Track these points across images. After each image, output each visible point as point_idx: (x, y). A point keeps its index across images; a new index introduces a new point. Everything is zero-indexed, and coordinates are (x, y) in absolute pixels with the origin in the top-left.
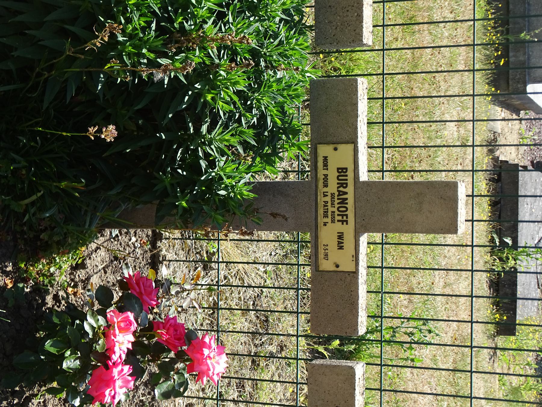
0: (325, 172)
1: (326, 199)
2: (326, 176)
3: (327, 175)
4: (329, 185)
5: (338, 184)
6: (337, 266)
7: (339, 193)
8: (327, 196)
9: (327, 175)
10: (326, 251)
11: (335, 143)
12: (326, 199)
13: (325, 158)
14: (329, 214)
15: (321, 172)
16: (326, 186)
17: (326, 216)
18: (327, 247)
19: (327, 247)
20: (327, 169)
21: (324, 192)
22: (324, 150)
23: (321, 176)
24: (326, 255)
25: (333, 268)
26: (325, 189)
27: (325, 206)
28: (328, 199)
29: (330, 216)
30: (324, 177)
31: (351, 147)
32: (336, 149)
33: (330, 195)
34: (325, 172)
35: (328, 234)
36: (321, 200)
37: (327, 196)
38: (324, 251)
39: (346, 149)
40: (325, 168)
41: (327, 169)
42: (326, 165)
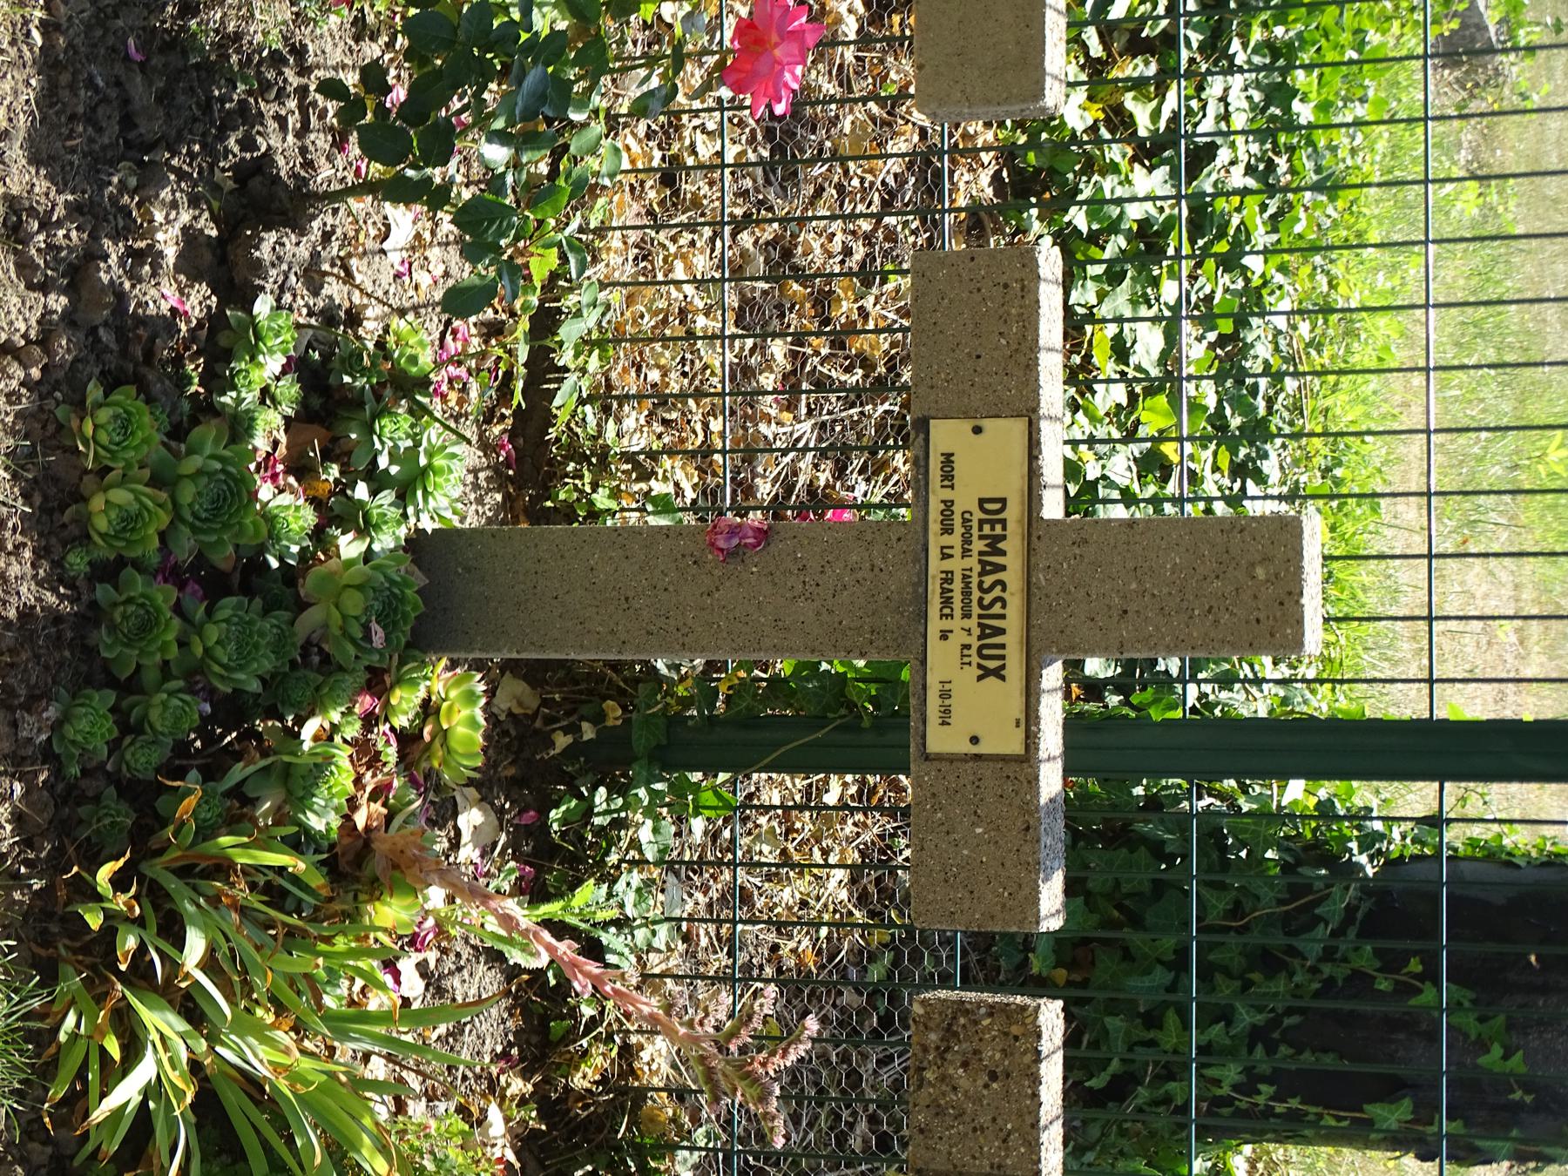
0: (947, 494)
1: (948, 565)
2: (949, 504)
7: (983, 568)
10: (947, 702)
11: (976, 414)
12: (948, 565)
13: (948, 459)
16: (947, 530)
20: (952, 487)
24: (946, 711)
25: (967, 748)
26: (947, 540)
27: (945, 580)
29: (958, 613)
30: (942, 506)
31: (1018, 427)
32: (977, 430)
34: (947, 494)
36: (935, 565)
38: (940, 701)
39: (1006, 432)
41: (952, 487)
42: (948, 477)
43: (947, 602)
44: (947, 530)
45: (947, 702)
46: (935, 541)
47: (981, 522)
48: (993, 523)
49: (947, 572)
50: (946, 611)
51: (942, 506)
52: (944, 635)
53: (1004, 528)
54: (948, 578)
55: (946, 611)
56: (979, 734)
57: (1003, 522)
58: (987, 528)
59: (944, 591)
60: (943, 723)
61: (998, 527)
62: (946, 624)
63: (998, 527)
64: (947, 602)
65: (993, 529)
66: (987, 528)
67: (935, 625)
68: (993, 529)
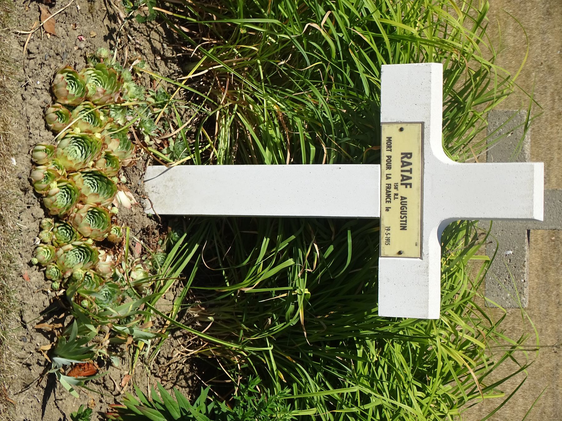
0: (389, 153)
1: (389, 181)
2: (389, 157)
3: (391, 156)
4: (392, 167)
8: (390, 178)
9: (391, 156)
10: (388, 236)
12: (389, 181)
13: (389, 139)
14: (392, 197)
16: (389, 167)
18: (389, 232)
20: (391, 150)
21: (387, 175)
24: (388, 240)
26: (388, 172)
30: (387, 158)
32: (401, 130)
34: (389, 153)
37: (390, 178)
38: (385, 236)
40: (388, 149)
41: (391, 150)
42: (389, 146)
43: (388, 196)
44: (389, 167)
45: (388, 236)
49: (388, 184)
50: (388, 200)
51: (387, 158)
52: (387, 209)
55: (388, 200)
59: (387, 192)
62: (388, 205)
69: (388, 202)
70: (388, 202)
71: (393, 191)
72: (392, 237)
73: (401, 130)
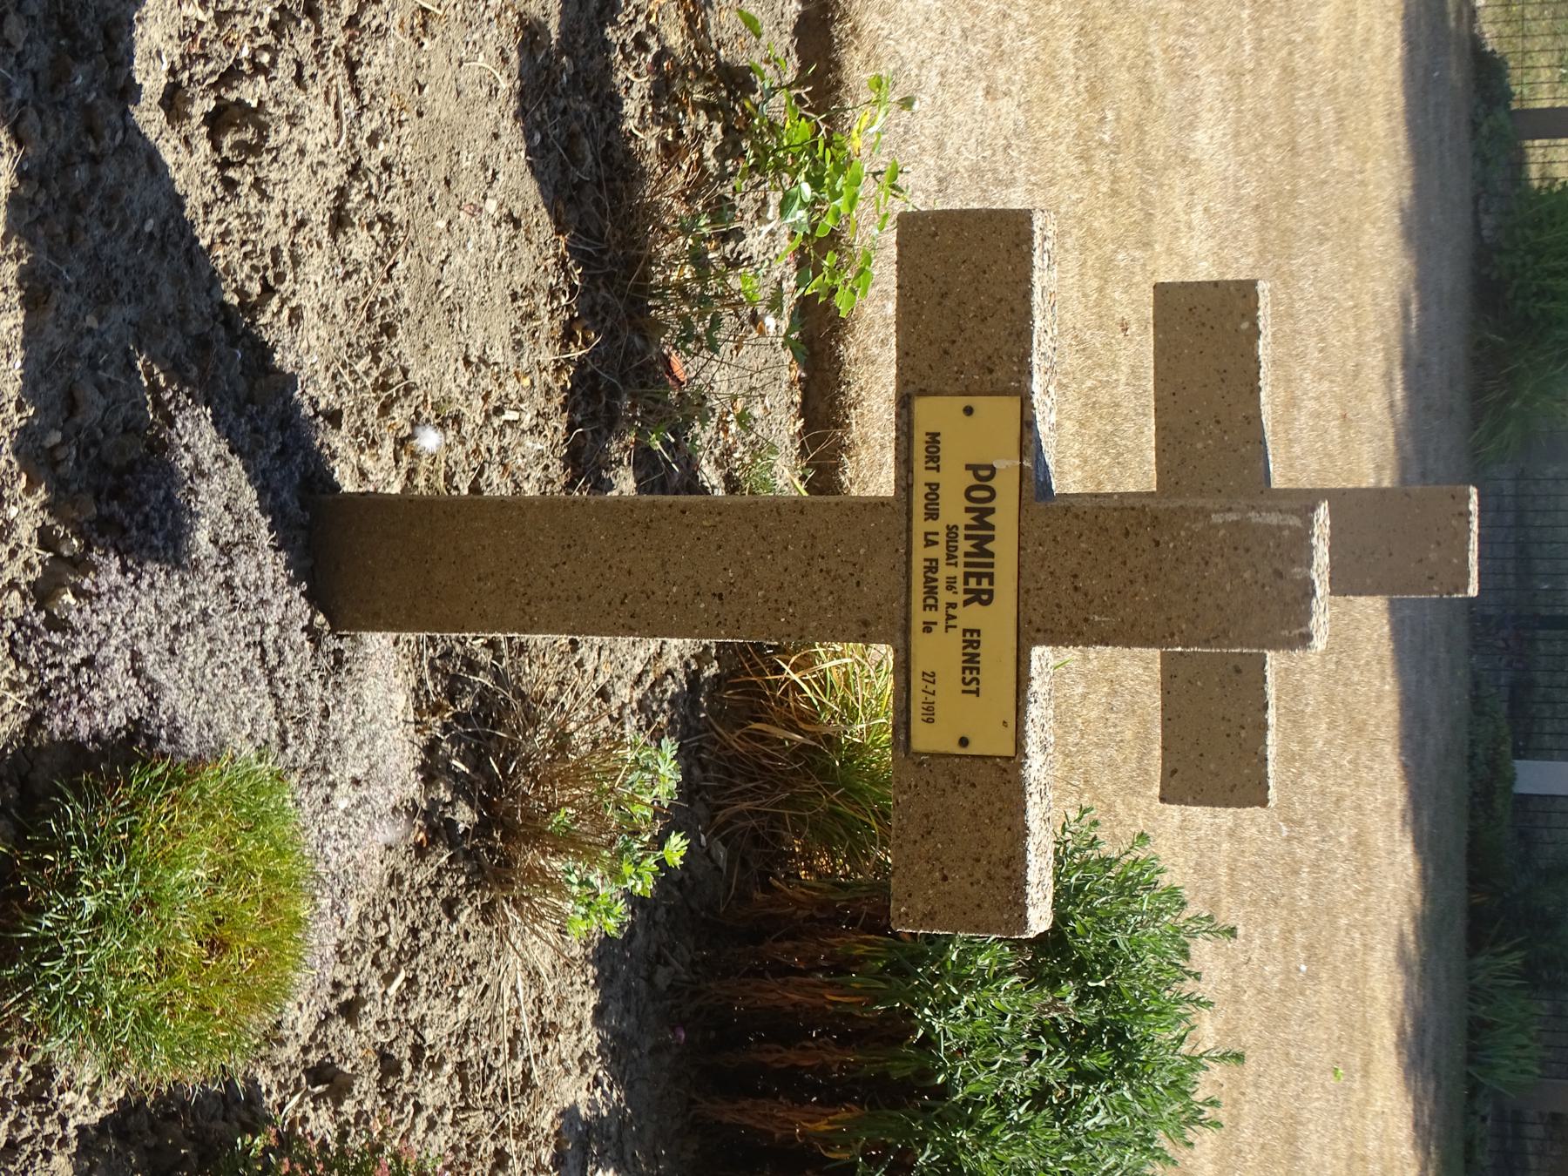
0: (933, 477)
1: (933, 552)
2: (933, 487)
5: (968, 510)
6: (964, 742)
8: (936, 543)
10: (931, 698)
12: (933, 552)
13: (934, 438)
15: (922, 476)
16: (932, 514)
17: (931, 603)
18: (931, 688)
19: (931, 688)
20: (938, 469)
21: (927, 534)
22: (929, 412)
23: (919, 492)
26: (931, 526)
28: (939, 552)
30: (927, 490)
33: (942, 539)
34: (933, 477)
35: (937, 652)
36: (920, 554)
37: (936, 543)
40: (931, 464)
41: (938, 469)
42: (933, 458)
43: (931, 591)
45: (931, 698)
46: (920, 525)
47: (967, 576)
48: (979, 577)
49: (931, 560)
52: (928, 628)
53: (991, 583)
54: (932, 565)
56: (969, 736)
57: (991, 577)
58: (973, 583)
59: (928, 580)
60: (930, 721)
61: (985, 584)
62: (930, 616)
63: (985, 582)
64: (931, 591)
65: (979, 583)
66: (973, 583)
67: (919, 616)
68: (979, 583)
69: (931, 607)
70: (931, 607)
71: (944, 572)
72: (939, 701)
73: (969, 411)
